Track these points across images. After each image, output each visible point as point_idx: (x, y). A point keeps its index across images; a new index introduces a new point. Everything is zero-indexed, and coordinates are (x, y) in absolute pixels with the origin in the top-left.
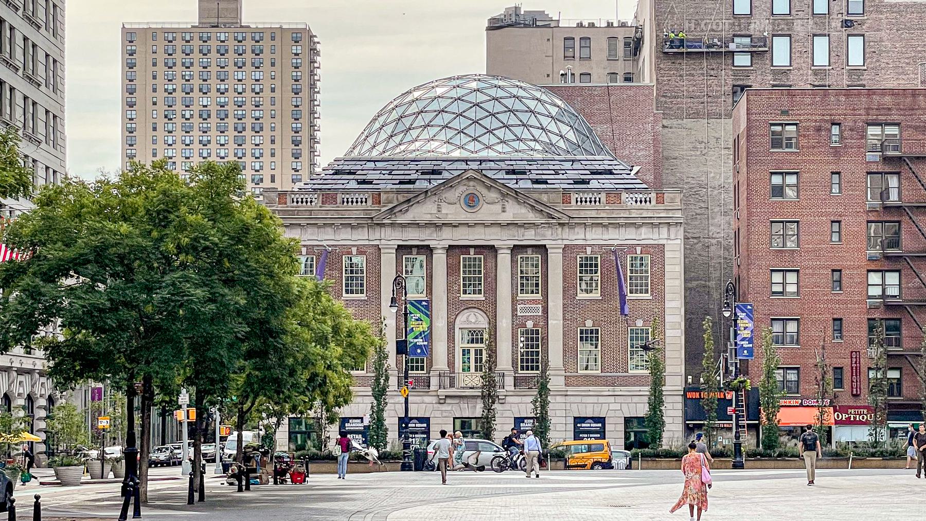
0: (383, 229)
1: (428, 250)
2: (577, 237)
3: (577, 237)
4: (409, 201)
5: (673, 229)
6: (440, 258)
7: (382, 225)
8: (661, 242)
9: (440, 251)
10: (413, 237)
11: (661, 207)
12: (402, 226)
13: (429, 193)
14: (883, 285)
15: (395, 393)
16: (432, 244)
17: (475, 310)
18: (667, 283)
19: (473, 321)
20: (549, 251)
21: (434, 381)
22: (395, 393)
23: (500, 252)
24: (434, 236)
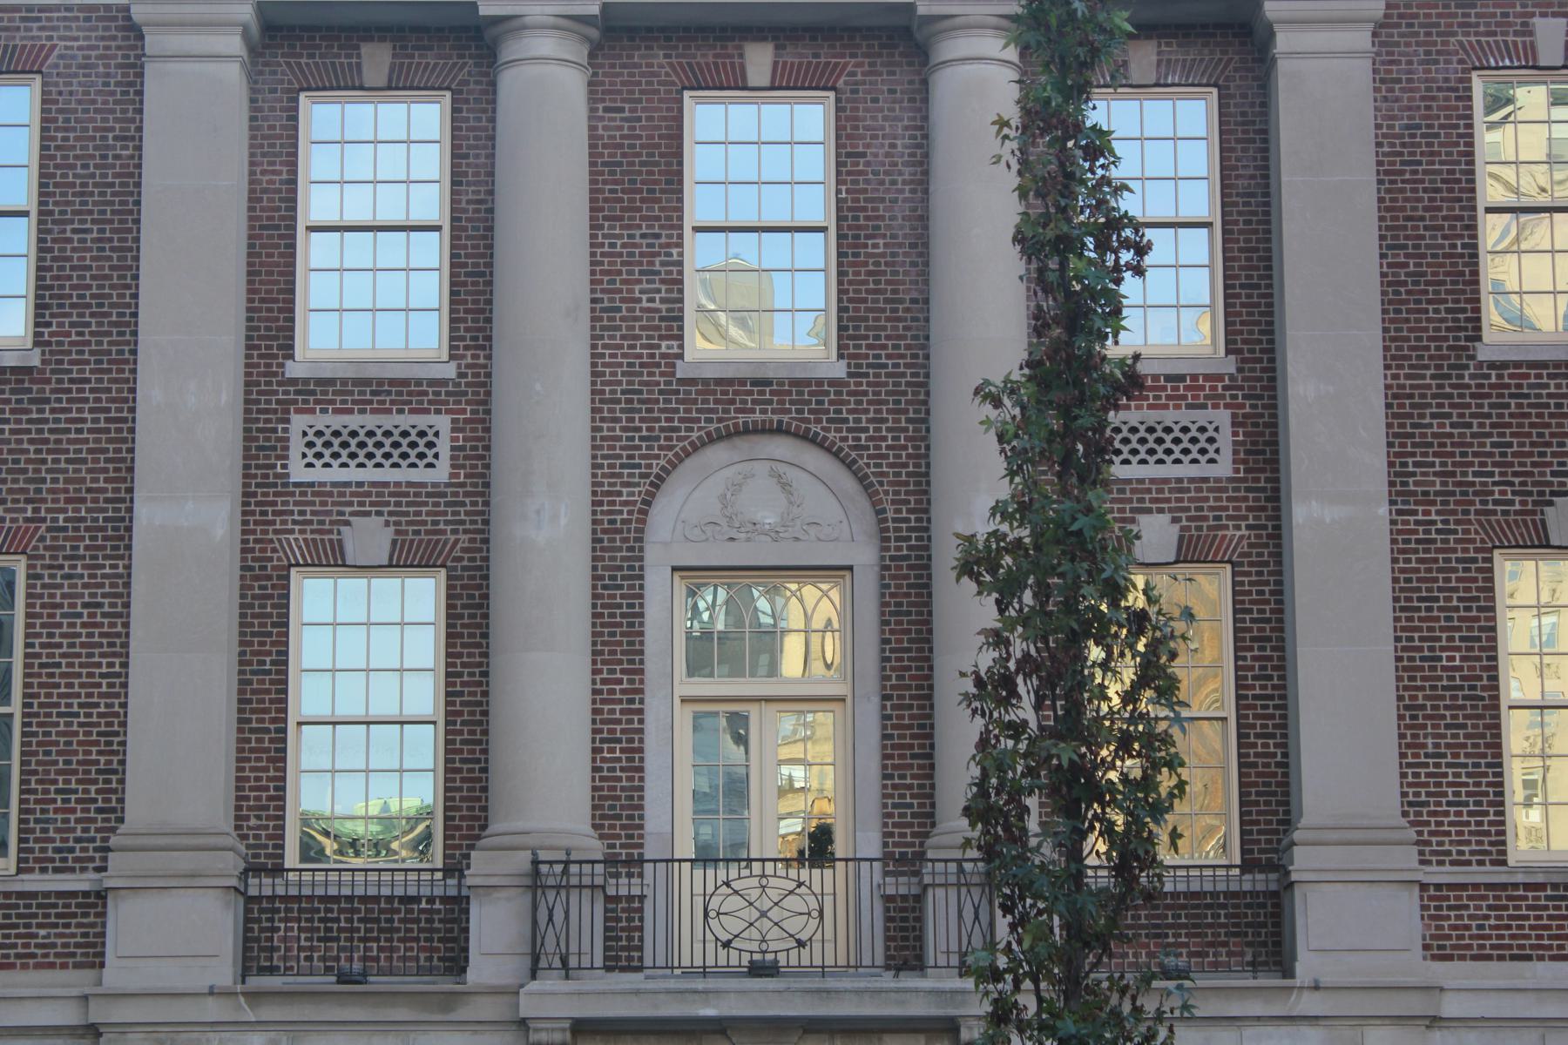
9: (546, 45)
15: (214, 1010)
17: (781, 447)
19: (769, 519)
20: (1284, 41)
21: (494, 930)
22: (214, 1010)
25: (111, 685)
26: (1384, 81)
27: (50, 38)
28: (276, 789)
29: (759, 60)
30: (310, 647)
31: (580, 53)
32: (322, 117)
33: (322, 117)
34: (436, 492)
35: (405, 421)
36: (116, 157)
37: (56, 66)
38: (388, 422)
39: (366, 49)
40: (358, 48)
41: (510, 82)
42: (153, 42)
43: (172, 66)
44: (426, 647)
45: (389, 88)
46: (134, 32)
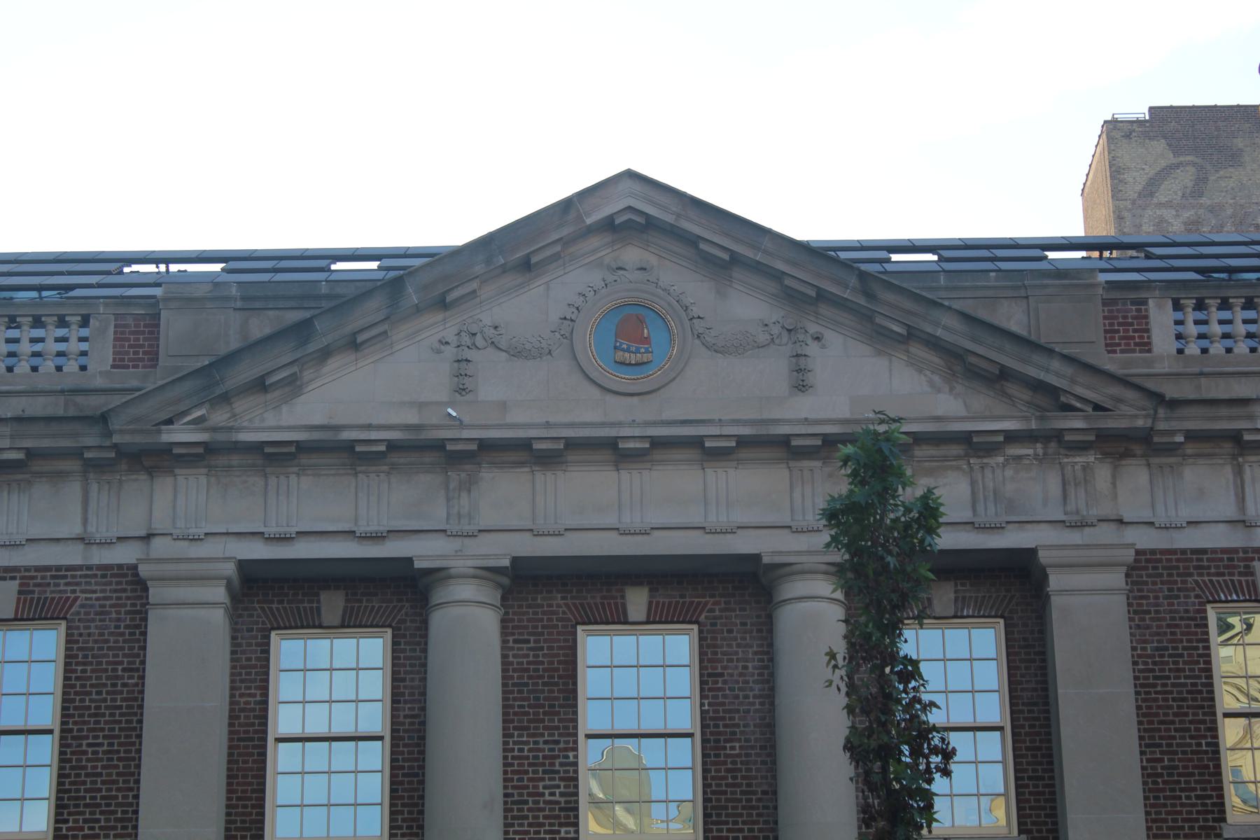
0: (163, 488)
4: (302, 331)
6: (470, 629)
7: (154, 460)
9: (466, 590)
10: (321, 519)
12: (276, 457)
13: (412, 296)
16: (423, 552)
20: (1056, 581)
25: (124, 812)
26: (1137, 612)
27: (74, 591)
28: (258, 784)
29: (637, 601)
30: (284, 687)
31: (494, 596)
32: (288, 650)
33: (288, 650)
36: (124, 685)
37: (78, 613)
39: (324, 596)
40: (318, 595)
41: (438, 620)
42: (155, 593)
43: (172, 612)
44: (376, 685)
45: (343, 626)
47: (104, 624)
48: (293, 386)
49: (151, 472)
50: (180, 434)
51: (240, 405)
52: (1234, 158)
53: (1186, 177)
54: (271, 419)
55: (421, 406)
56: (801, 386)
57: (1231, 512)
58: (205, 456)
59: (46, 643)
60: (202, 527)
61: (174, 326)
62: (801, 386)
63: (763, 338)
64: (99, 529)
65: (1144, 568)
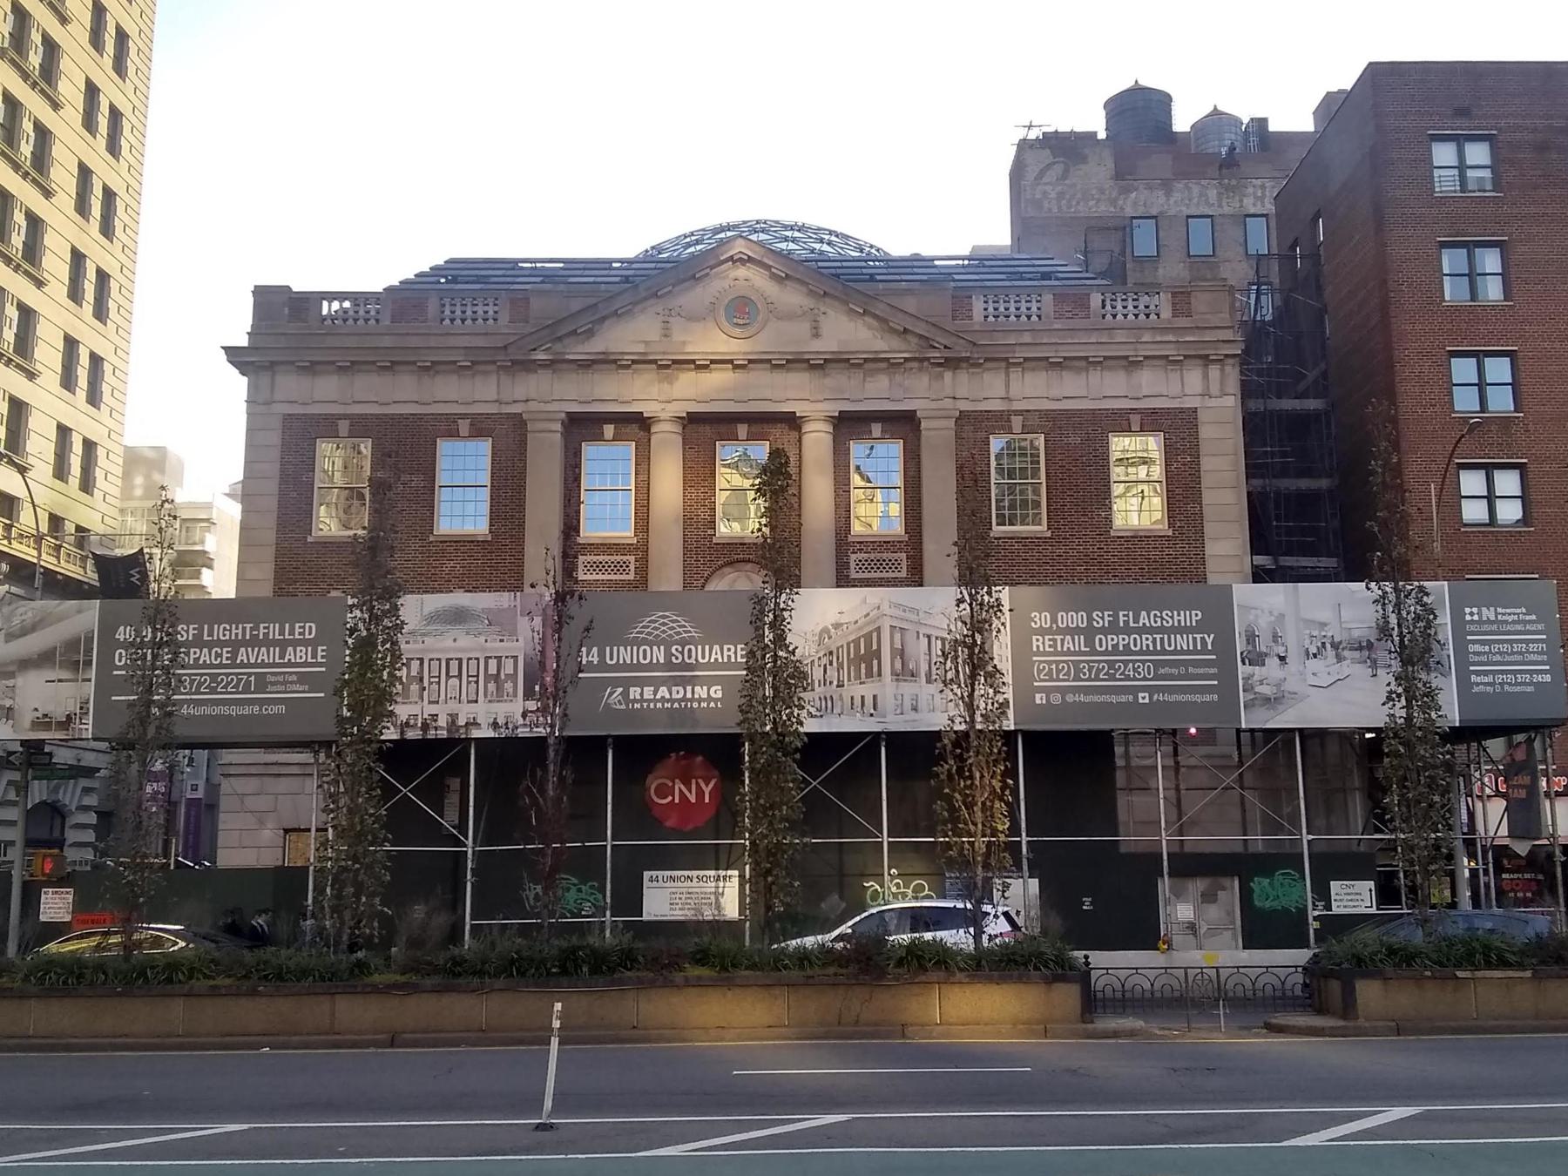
1: (637, 425)
2: (987, 390)
3: (987, 390)
5: (1214, 371)
7: (526, 366)
8: (1189, 403)
11: (1183, 322)
14: (1462, 167)
16: (648, 409)
18: (1208, 497)
23: (806, 428)
24: (654, 390)
29: (742, 430)
31: (678, 429)
32: (589, 451)
33: (589, 451)
34: (629, 582)
35: (619, 558)
38: (613, 558)
46: (524, 423)
47: (509, 440)
48: (590, 333)
49: (528, 371)
50: (541, 356)
51: (566, 341)
52: (1084, 159)
53: (1059, 169)
54: (580, 349)
55: (646, 343)
56: (817, 335)
57: (1003, 394)
58: (553, 365)
59: (485, 447)
60: (550, 396)
61: (536, 304)
62: (817, 335)
63: (800, 312)
64: (505, 397)
65: (963, 418)
